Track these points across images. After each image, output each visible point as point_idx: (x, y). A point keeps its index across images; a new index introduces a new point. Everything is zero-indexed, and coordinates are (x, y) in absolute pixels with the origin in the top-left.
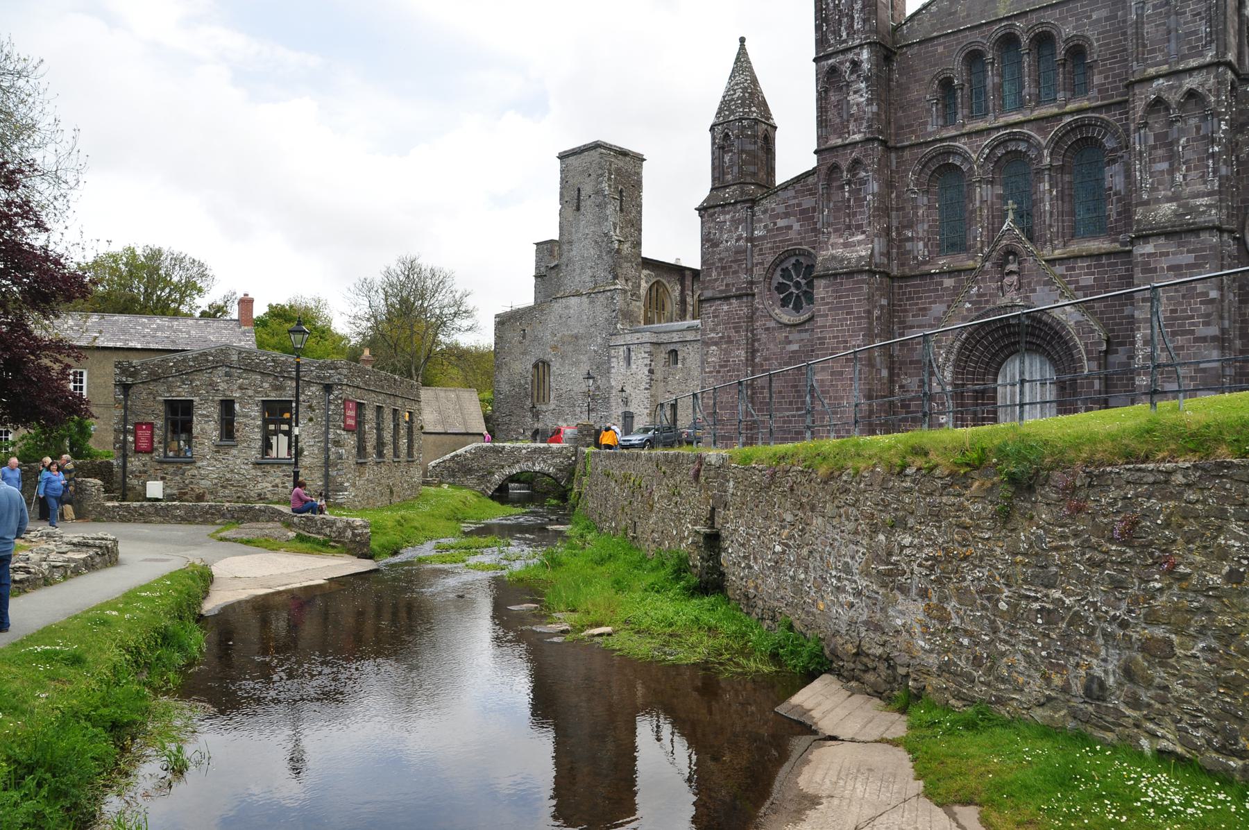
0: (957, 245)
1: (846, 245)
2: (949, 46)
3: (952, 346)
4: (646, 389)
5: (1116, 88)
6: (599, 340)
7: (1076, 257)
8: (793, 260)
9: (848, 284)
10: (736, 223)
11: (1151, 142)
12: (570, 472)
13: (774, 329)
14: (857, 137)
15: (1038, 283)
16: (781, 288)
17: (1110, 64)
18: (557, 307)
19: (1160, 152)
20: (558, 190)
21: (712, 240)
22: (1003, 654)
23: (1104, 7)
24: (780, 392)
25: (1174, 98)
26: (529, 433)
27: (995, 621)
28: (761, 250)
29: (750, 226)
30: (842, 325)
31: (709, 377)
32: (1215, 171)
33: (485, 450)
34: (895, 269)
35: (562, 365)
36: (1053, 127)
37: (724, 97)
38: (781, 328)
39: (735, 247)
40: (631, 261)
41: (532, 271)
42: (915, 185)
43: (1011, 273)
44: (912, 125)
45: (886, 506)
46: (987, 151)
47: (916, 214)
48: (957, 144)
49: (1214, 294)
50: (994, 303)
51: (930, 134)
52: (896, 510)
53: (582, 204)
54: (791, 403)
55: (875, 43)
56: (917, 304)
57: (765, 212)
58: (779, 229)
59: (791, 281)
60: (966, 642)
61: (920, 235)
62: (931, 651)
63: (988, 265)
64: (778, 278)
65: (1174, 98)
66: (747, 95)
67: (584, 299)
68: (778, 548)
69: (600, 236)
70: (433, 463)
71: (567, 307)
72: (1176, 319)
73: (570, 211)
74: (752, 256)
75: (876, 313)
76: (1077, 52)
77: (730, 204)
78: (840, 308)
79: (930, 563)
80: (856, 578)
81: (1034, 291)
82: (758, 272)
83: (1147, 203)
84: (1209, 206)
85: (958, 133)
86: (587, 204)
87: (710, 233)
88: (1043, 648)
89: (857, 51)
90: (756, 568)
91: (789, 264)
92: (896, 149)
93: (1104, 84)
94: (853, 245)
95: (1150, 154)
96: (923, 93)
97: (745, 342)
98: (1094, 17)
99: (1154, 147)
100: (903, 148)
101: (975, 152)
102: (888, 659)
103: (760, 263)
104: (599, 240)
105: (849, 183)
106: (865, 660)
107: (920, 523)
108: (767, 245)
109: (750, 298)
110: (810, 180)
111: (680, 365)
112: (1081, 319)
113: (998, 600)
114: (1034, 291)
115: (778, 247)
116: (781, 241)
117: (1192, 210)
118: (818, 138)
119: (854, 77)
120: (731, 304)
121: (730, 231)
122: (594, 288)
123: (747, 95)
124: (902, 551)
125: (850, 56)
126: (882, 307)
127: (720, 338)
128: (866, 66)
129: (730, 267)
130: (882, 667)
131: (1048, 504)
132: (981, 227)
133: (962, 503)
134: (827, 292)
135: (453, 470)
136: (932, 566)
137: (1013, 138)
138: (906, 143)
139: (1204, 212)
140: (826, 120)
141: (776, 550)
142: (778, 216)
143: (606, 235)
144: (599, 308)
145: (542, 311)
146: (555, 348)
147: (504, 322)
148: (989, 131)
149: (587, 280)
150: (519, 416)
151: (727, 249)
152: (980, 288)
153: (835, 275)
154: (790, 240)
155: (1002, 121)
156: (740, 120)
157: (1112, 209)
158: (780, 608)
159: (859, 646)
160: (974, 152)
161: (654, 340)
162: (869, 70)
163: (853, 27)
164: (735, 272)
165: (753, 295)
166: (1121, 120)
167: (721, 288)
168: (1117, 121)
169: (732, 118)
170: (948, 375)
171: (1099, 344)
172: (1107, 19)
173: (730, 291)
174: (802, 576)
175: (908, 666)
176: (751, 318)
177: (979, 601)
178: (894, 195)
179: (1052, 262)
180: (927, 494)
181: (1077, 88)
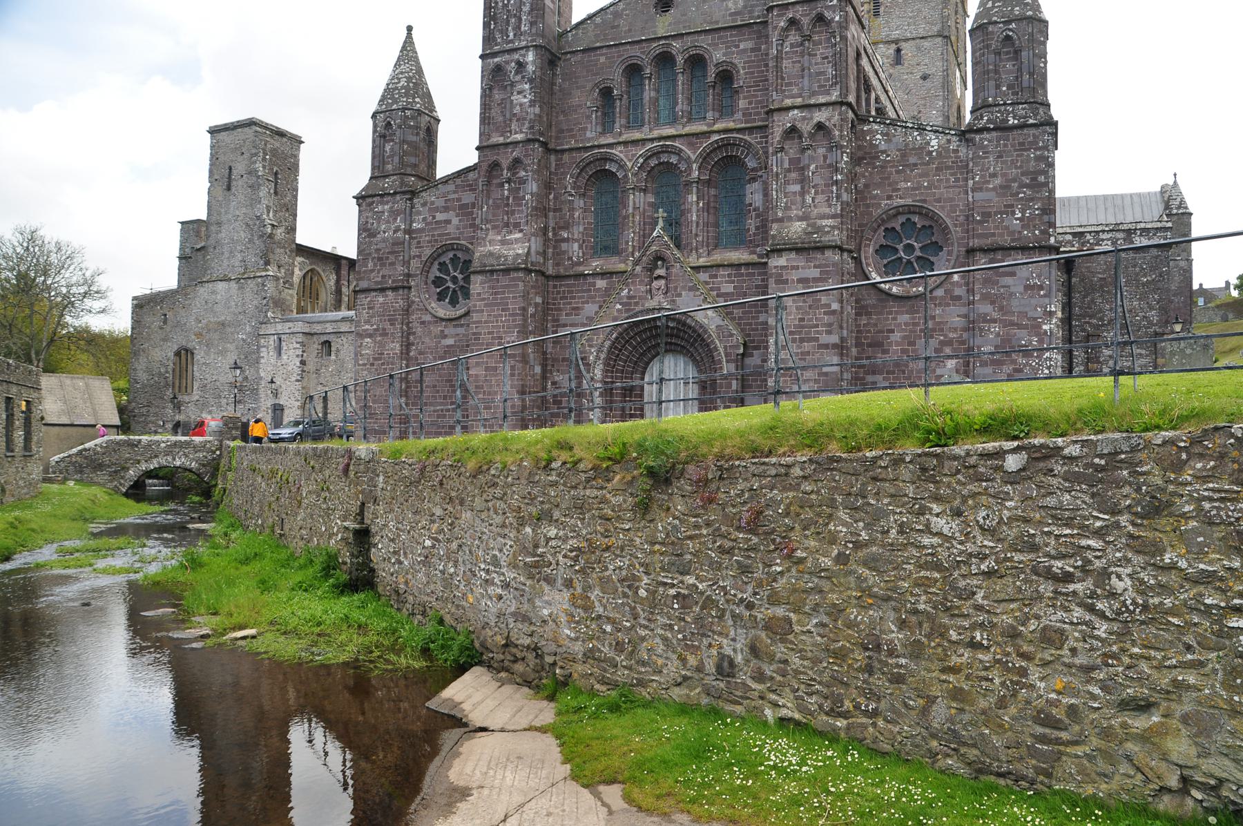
0: (610, 248)
2: (609, 58)
3: (602, 345)
4: (298, 381)
5: (758, 114)
6: (248, 329)
7: (718, 266)
8: (451, 255)
9: (504, 280)
10: (394, 214)
11: (786, 165)
12: (214, 467)
13: (429, 322)
14: (519, 137)
15: (683, 288)
16: (438, 282)
17: (754, 91)
18: (203, 291)
19: (794, 175)
20: (208, 167)
21: (369, 230)
22: (643, 639)
23: (751, 39)
24: (435, 386)
25: (806, 128)
26: (169, 426)
27: (635, 607)
28: (419, 242)
29: (408, 218)
30: (497, 321)
31: (362, 370)
32: (838, 197)
33: (118, 443)
34: (551, 268)
35: (207, 353)
36: (701, 143)
37: (388, 85)
38: (436, 322)
39: (393, 238)
40: (285, 248)
41: (176, 252)
42: (573, 188)
43: (659, 277)
44: (572, 130)
45: (532, 499)
46: (641, 160)
47: (572, 216)
48: (613, 151)
49: (835, 306)
50: (643, 306)
51: (589, 140)
52: (542, 502)
53: (234, 183)
54: (445, 397)
55: (541, 47)
56: (570, 303)
57: (424, 205)
59: (448, 275)
60: (608, 628)
61: (576, 237)
62: (576, 639)
63: (638, 268)
64: (434, 272)
65: (806, 128)
66: (411, 85)
67: (233, 284)
68: (428, 543)
69: (251, 219)
70: (56, 458)
71: (213, 292)
72: (803, 327)
73: (219, 192)
74: (410, 248)
75: (531, 310)
76: (726, 76)
77: (389, 194)
78: (496, 304)
79: (574, 553)
80: (504, 570)
81: (680, 295)
82: (415, 265)
83: (781, 220)
84: (833, 227)
85: (615, 141)
86: (238, 184)
87: (367, 222)
88: (679, 632)
89: (523, 52)
90: (406, 563)
91: (446, 258)
92: (556, 151)
93: (748, 109)
94: (510, 242)
95: (785, 176)
96: (584, 99)
97: (400, 334)
98: (742, 47)
99: (789, 170)
100: (563, 151)
101: (630, 160)
102: (536, 649)
103: (418, 256)
104: (251, 223)
105: (509, 181)
106: (514, 650)
107: (565, 516)
108: (425, 238)
109: (406, 290)
110: (471, 175)
111: (333, 357)
112: (721, 323)
113: (638, 588)
114: (680, 295)
115: (436, 241)
116: (439, 235)
117: (819, 230)
118: (481, 135)
119: (518, 78)
120: (387, 296)
121: (388, 222)
122: (244, 273)
123: (411, 85)
124: (547, 543)
125: (516, 56)
126: (536, 305)
127: (375, 330)
128: (531, 68)
130: (530, 656)
131: (683, 496)
132: (633, 232)
133: (604, 496)
134: (484, 288)
135: (80, 466)
136: (577, 556)
137: (665, 150)
138: (566, 147)
139: (828, 232)
140: (489, 117)
141: (426, 545)
142: (437, 210)
143: (258, 218)
144: (248, 295)
145: (186, 295)
146: (199, 335)
147: (142, 305)
148: (644, 141)
149: (237, 264)
150: (158, 407)
151: (384, 240)
152: (630, 290)
153: (492, 272)
154: (448, 234)
155: (656, 133)
156: (404, 109)
157: (752, 224)
158: (430, 603)
159: (508, 637)
160: (630, 160)
161: (307, 330)
162: (534, 72)
163: (520, 29)
164: (392, 264)
165: (410, 288)
166: (761, 143)
167: (376, 279)
168: (757, 143)
169: (395, 107)
170: (598, 373)
171: (737, 347)
172: (752, 50)
173: (386, 282)
174: (452, 570)
175: (555, 655)
176: (407, 311)
177: (620, 589)
178: (551, 197)
179: (697, 269)
180: (572, 487)
181: (725, 110)
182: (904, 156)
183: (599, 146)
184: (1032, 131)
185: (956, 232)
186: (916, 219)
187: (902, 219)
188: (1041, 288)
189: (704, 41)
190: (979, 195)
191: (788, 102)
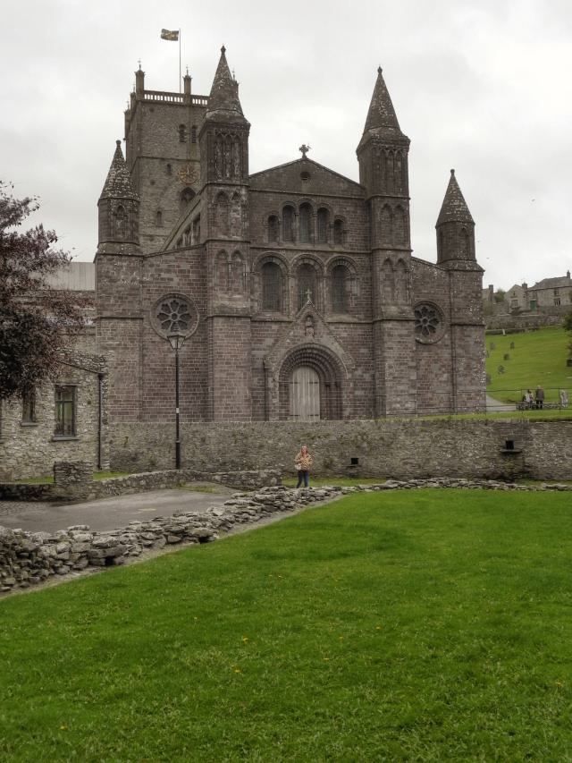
1: (230, 299)
8: (171, 300)
9: (238, 323)
13: (159, 342)
14: (239, 238)
16: (161, 316)
25: (395, 260)
58: (162, 279)
63: (299, 321)
64: (159, 310)
65: (395, 260)
76: (338, 223)
81: (322, 337)
83: (385, 305)
94: (235, 300)
108: (153, 288)
114: (322, 337)
117: (403, 312)
119: (233, 202)
125: (234, 189)
127: (119, 345)
129: (126, 298)
142: (161, 271)
148: (297, 251)
170: (277, 377)
172: (353, 212)
181: (340, 242)
182: (424, 277)
183: (271, 249)
184: (475, 273)
185: (447, 315)
186: (427, 307)
187: (422, 307)
188: (480, 343)
189: (329, 202)
190: (456, 300)
191: (385, 246)
